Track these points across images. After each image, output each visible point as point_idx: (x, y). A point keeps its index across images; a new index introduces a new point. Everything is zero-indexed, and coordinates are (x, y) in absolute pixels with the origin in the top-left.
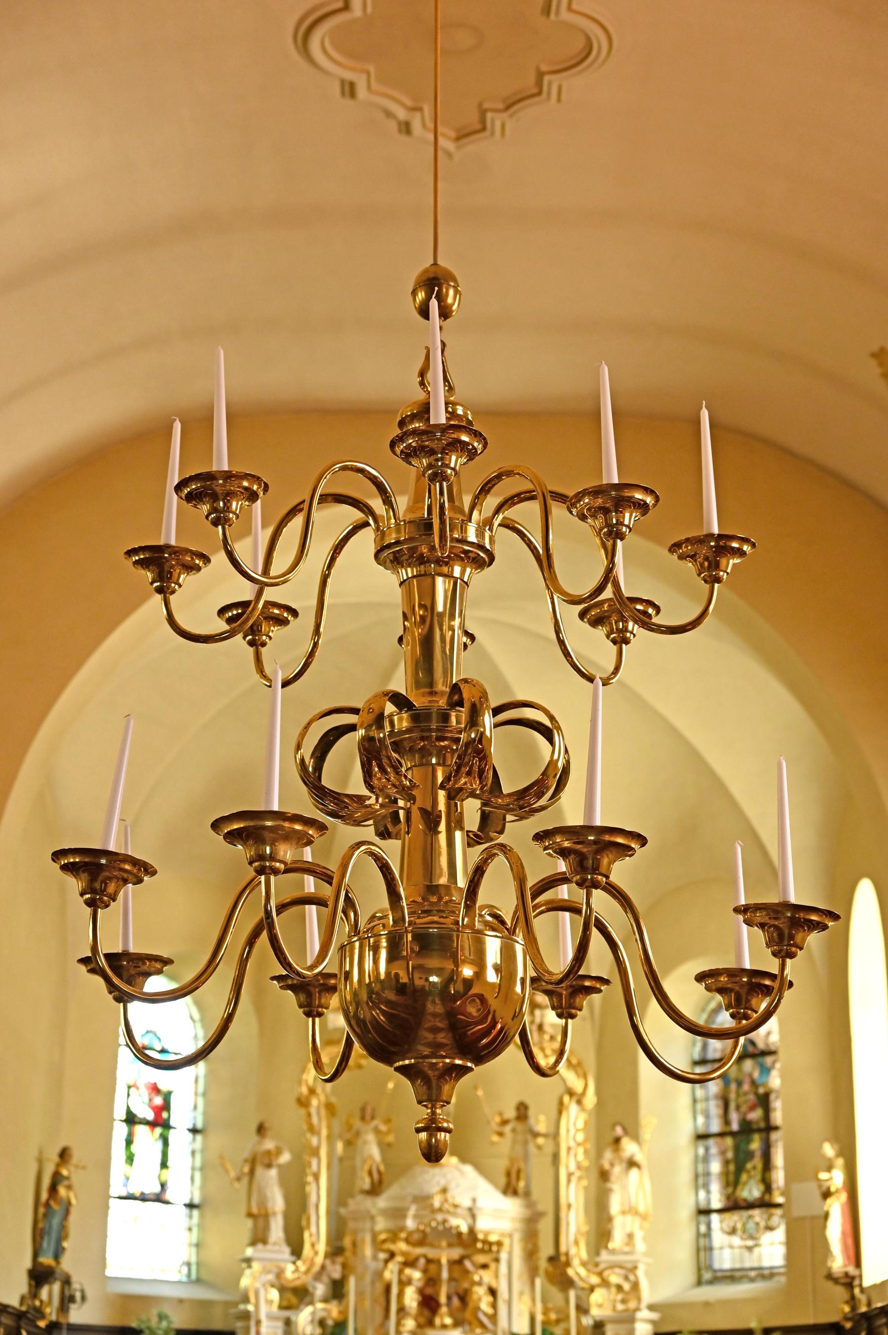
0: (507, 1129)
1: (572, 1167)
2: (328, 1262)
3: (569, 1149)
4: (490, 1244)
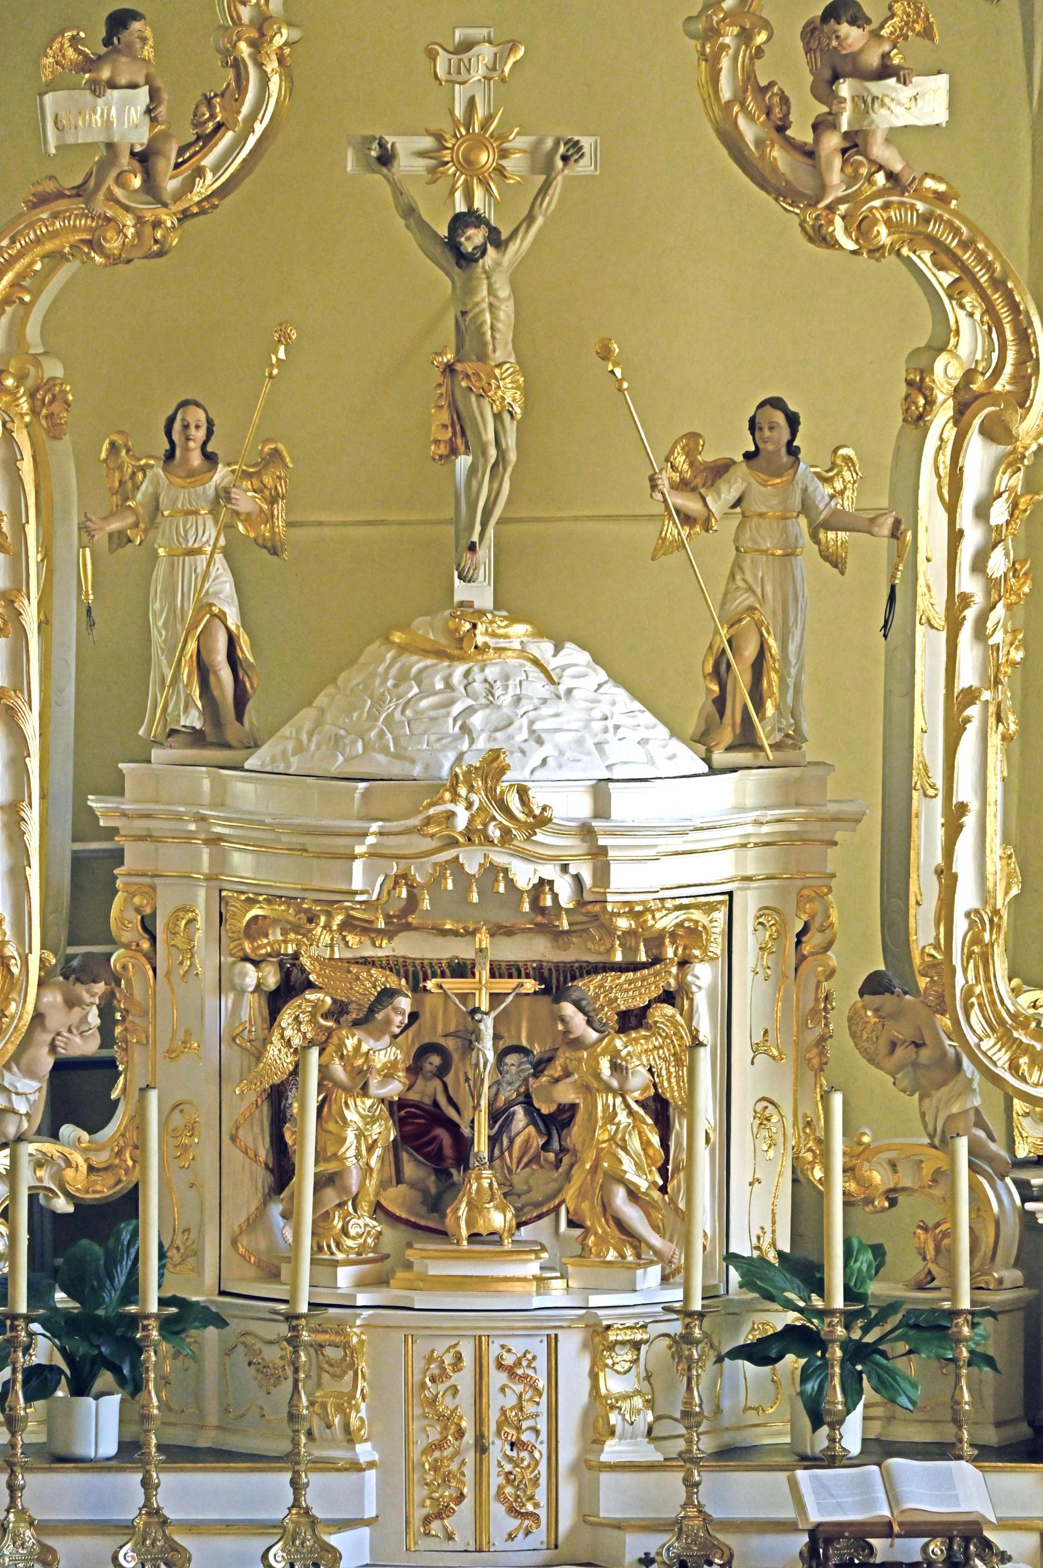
0: (718, 502)
1: (967, 676)
2: (53, 998)
3: (956, 604)
4: (656, 941)
